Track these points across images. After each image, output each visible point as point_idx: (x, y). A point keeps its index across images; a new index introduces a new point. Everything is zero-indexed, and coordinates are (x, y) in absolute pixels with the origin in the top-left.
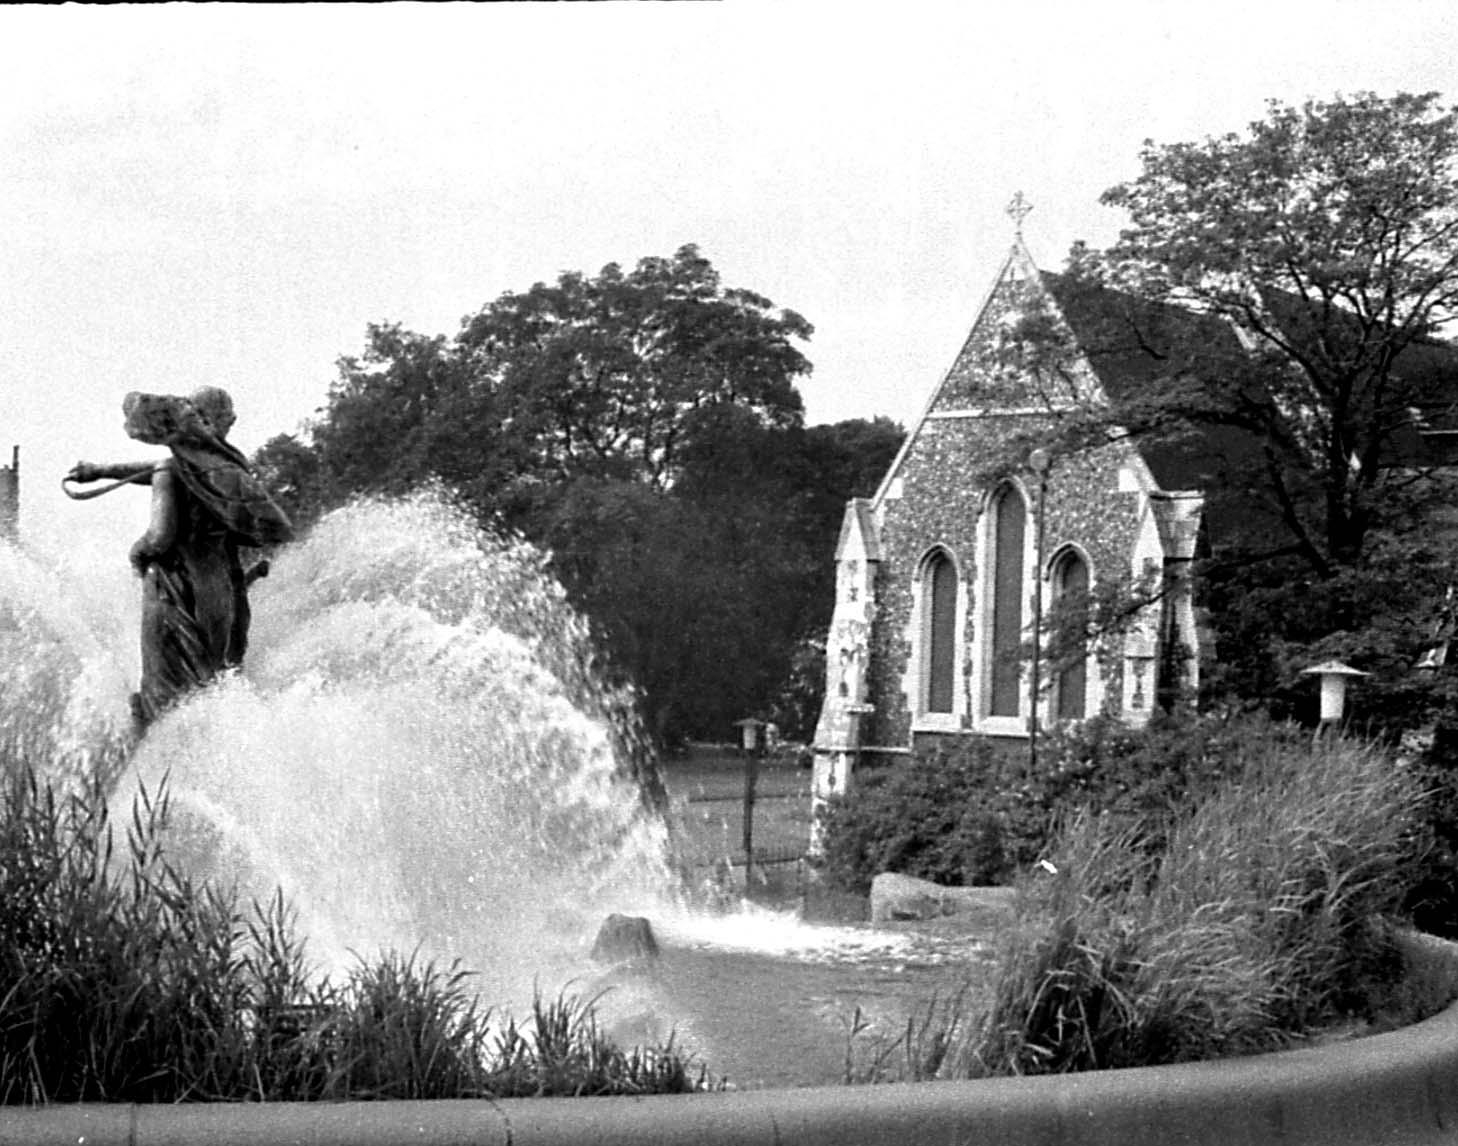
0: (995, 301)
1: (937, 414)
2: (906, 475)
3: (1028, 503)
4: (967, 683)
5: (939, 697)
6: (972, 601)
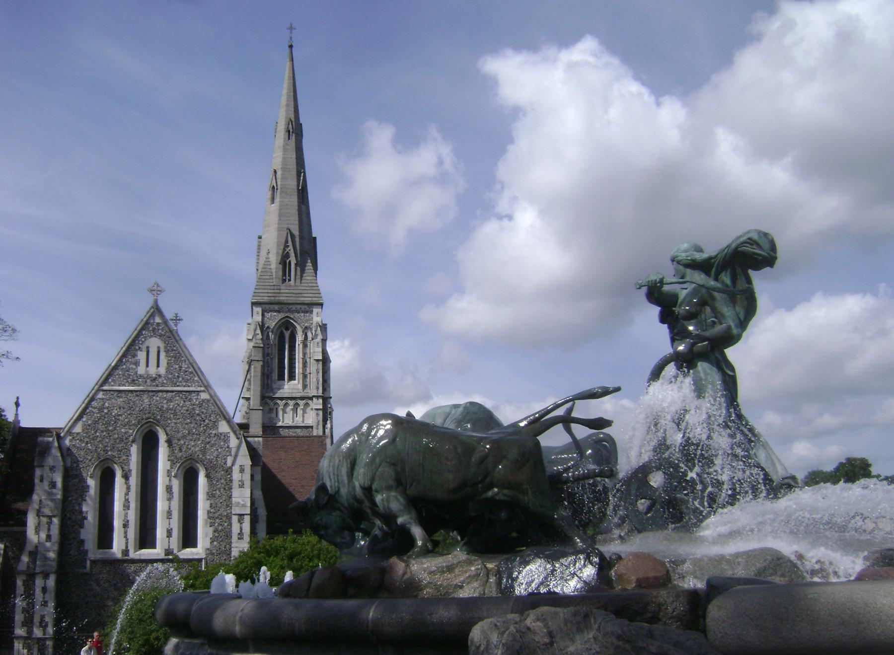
1: (105, 388)
2: (84, 419)
3: (162, 438)
4: (126, 533)
5: (105, 539)
6: (128, 488)
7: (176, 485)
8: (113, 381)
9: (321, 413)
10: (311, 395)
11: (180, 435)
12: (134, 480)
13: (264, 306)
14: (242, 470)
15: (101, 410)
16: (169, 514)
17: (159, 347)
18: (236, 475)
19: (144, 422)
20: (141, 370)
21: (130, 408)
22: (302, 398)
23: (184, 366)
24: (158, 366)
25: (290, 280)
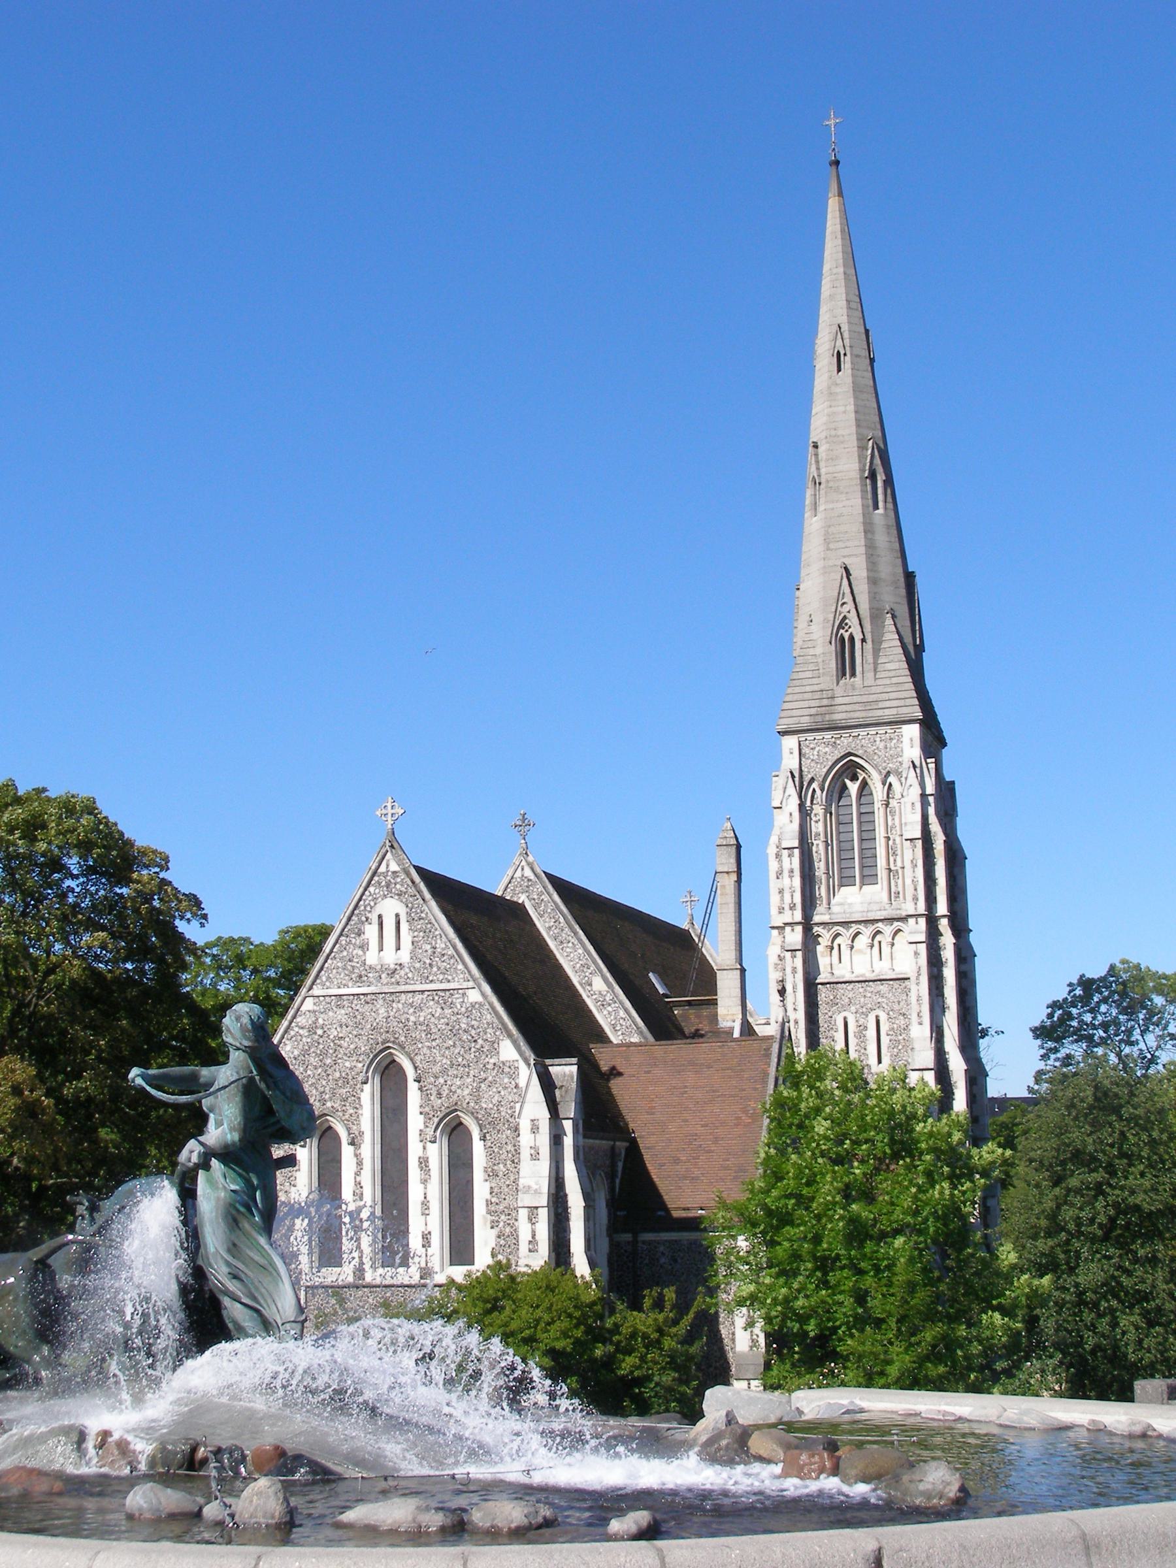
0: (371, 889)
3: (410, 1073)
6: (360, 1164)
7: (436, 1154)
8: (329, 978)
9: (923, 948)
10: (904, 914)
11: (436, 1069)
12: (369, 1149)
13: (803, 737)
14: (535, 1129)
15: (312, 1030)
16: (425, 1204)
17: (397, 915)
18: (526, 1139)
19: (380, 1047)
20: (372, 957)
21: (357, 1025)
22: (890, 920)
23: (440, 945)
24: (398, 948)
25: (853, 674)
